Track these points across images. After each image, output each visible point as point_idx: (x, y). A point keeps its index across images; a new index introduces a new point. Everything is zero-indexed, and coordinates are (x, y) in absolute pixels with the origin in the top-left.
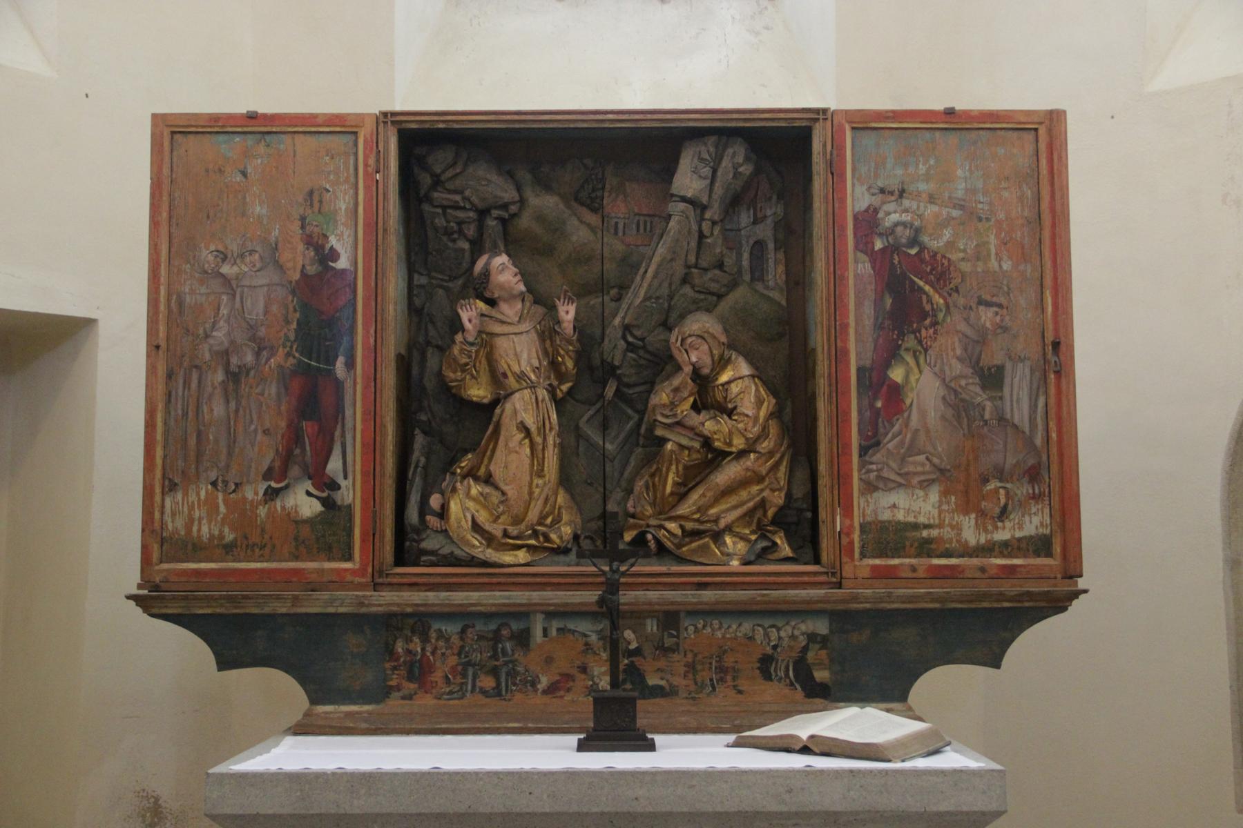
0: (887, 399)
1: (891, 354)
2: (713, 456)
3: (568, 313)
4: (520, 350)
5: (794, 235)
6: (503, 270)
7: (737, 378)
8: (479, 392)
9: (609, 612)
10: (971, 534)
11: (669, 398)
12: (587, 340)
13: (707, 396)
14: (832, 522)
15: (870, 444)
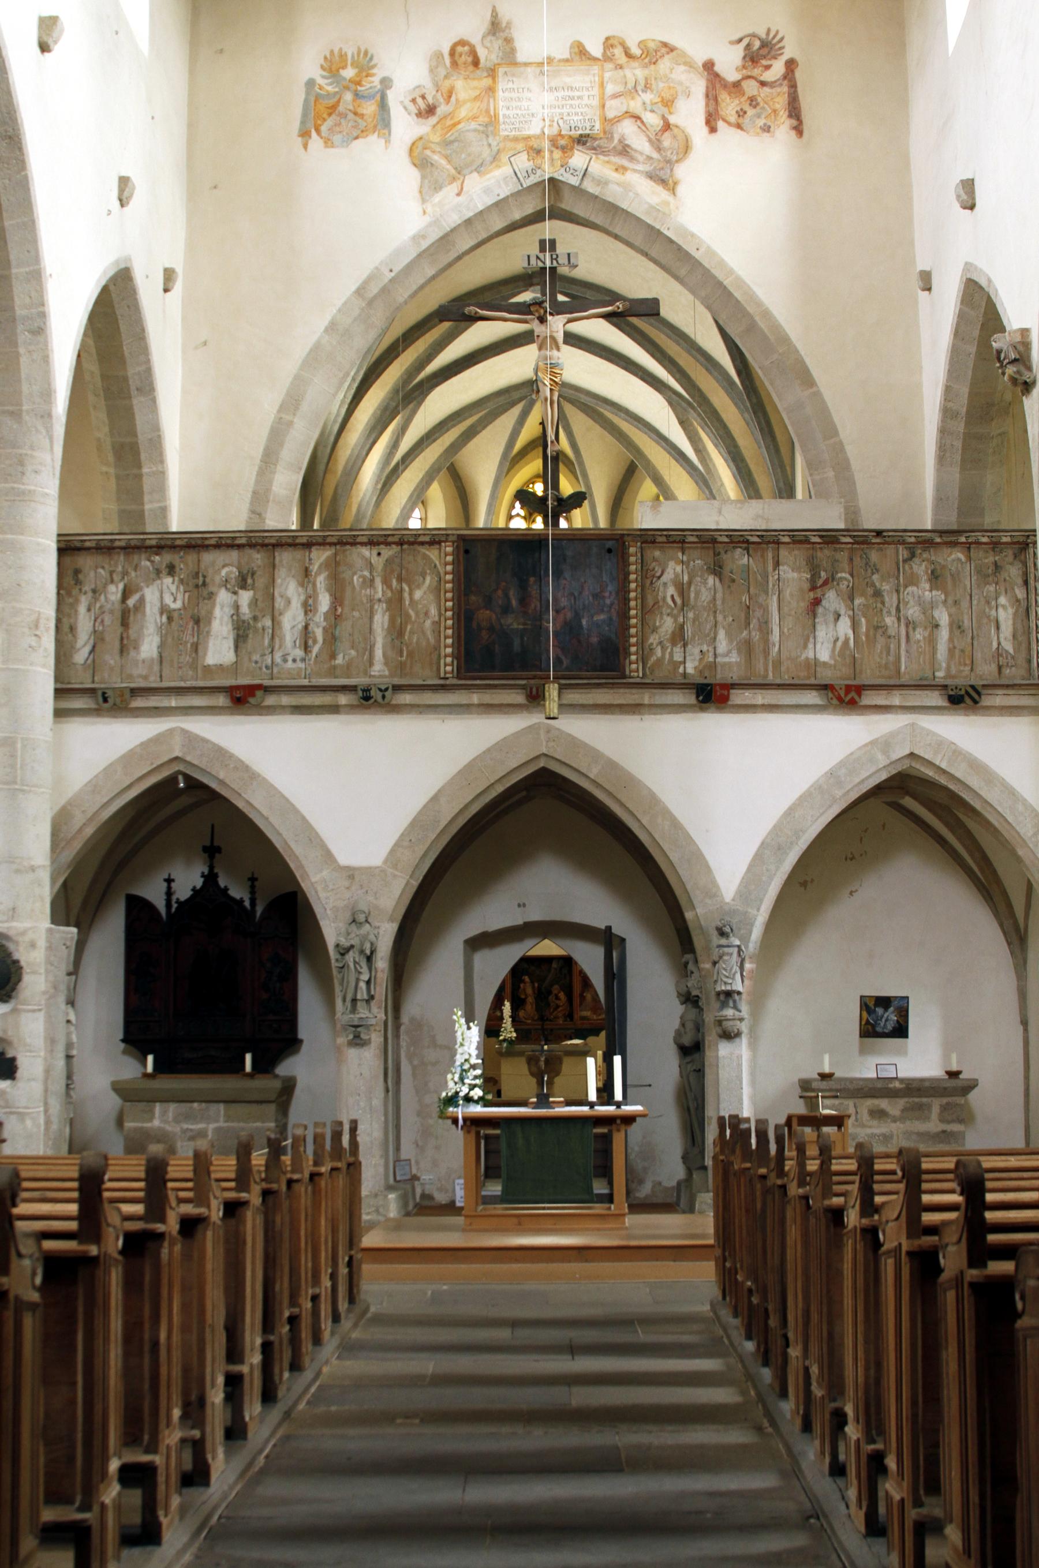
0: (582, 997)
1: (583, 992)
2: (558, 1006)
3: (536, 985)
4: (529, 991)
5: (570, 972)
6: (526, 978)
7: (562, 995)
8: (523, 997)
9: (543, 1029)
10: (595, 1017)
11: (551, 998)
12: (539, 988)
13: (557, 998)
14: (576, 1017)
15: (581, 1004)
